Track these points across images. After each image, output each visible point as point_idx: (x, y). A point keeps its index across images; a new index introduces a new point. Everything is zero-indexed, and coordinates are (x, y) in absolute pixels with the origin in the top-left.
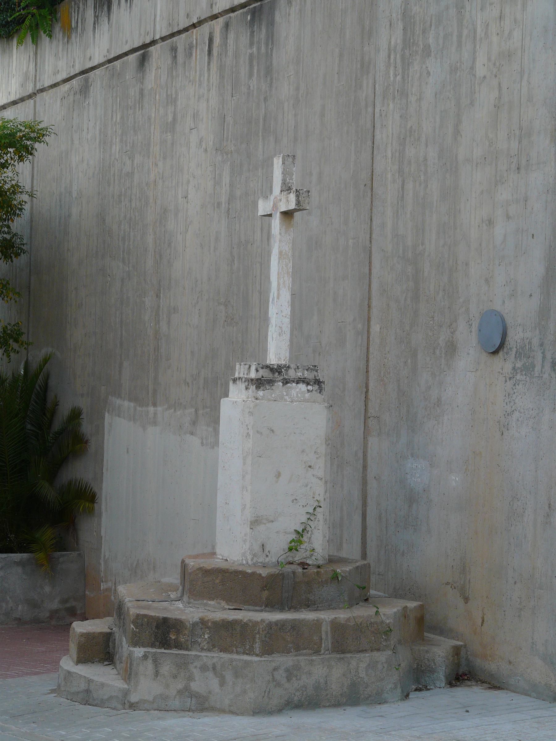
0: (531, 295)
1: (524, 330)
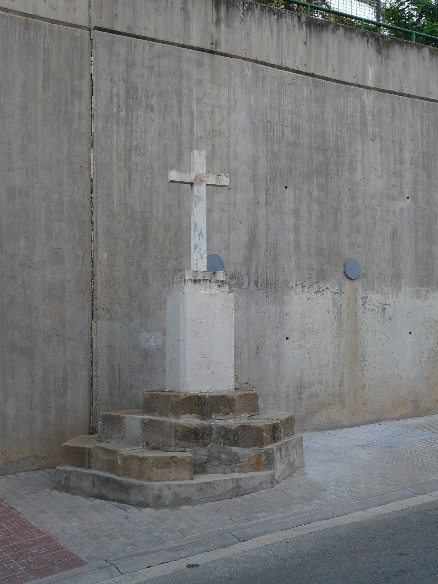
0: (239, 250)
1: (235, 266)
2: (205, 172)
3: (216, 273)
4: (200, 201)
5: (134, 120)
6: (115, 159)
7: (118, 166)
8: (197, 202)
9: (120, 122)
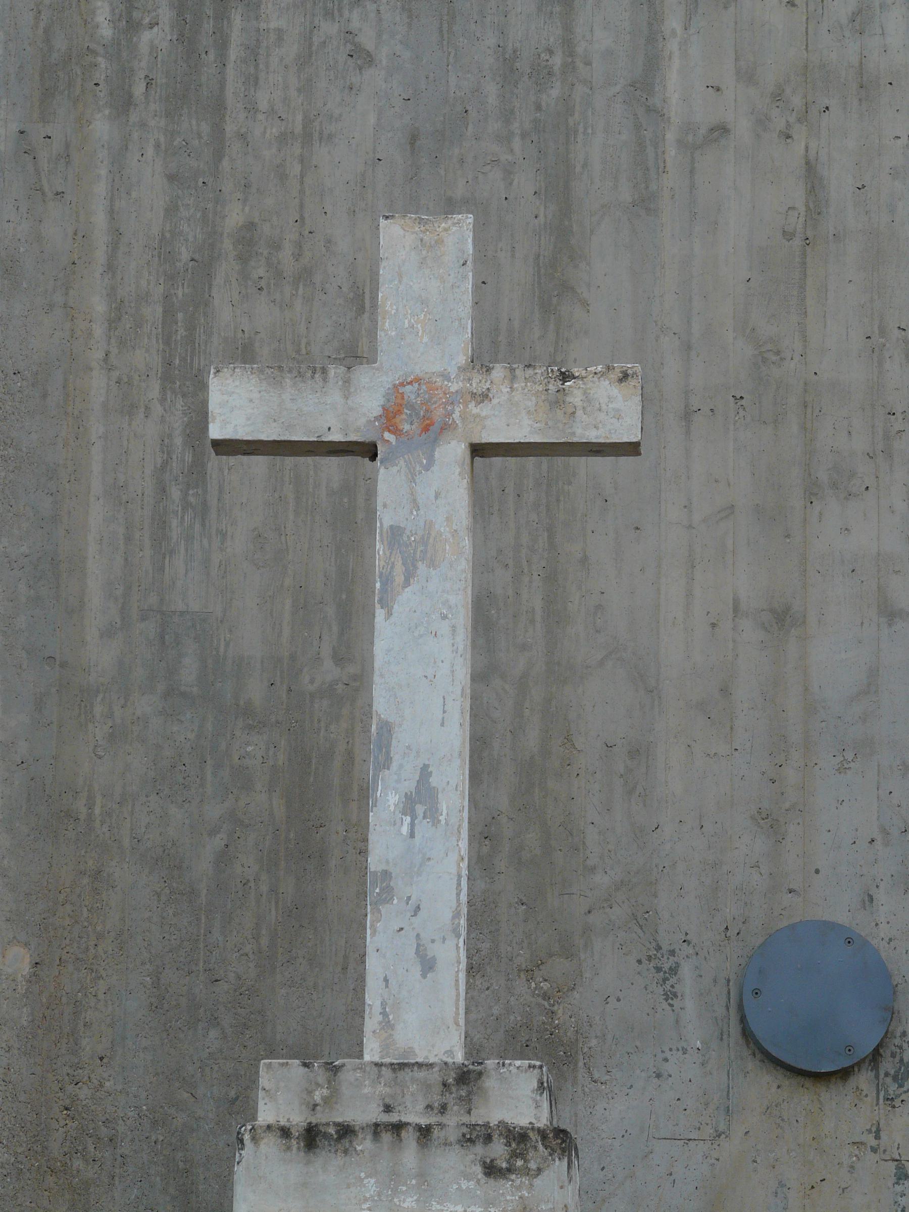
2: (462, 360)
3: (480, 1074)
4: (422, 567)
5: (230, 72)
6: (99, 331)
7: (115, 374)
8: (399, 579)
9: (139, 89)
